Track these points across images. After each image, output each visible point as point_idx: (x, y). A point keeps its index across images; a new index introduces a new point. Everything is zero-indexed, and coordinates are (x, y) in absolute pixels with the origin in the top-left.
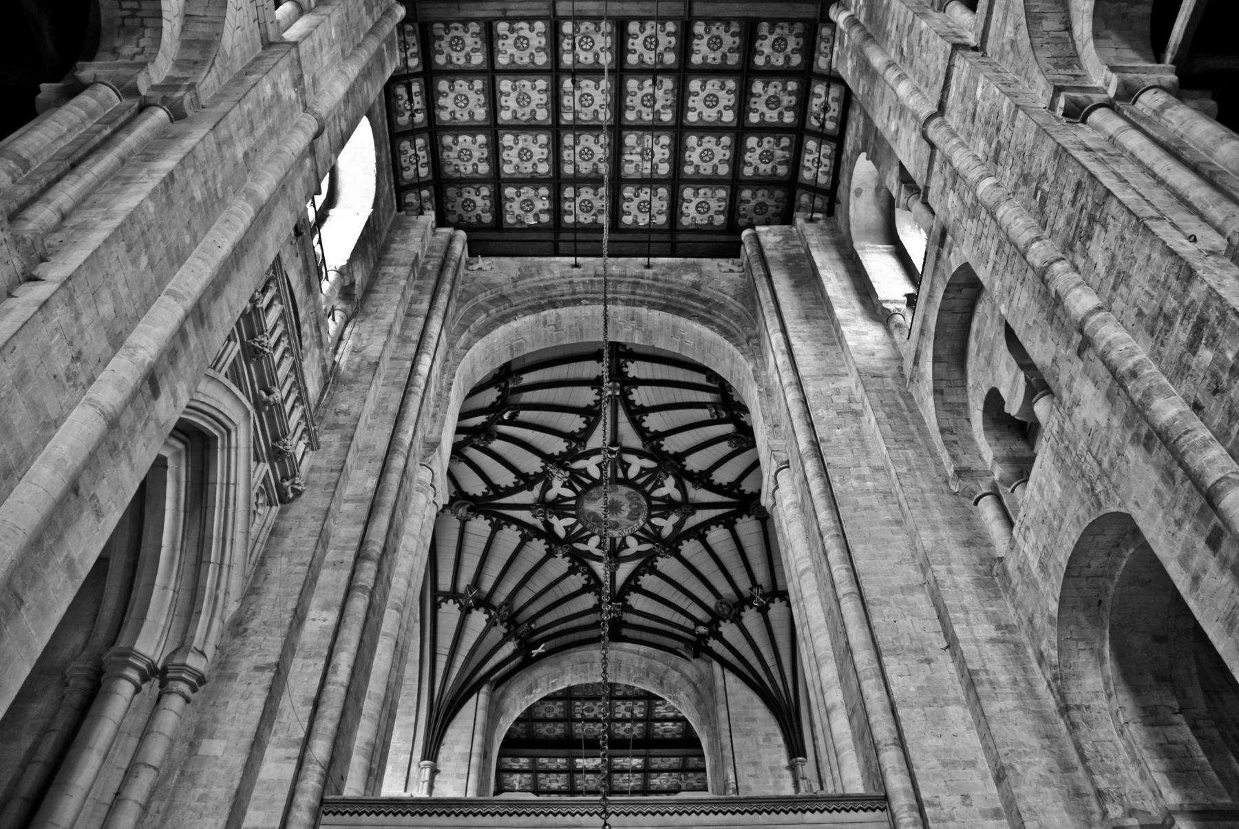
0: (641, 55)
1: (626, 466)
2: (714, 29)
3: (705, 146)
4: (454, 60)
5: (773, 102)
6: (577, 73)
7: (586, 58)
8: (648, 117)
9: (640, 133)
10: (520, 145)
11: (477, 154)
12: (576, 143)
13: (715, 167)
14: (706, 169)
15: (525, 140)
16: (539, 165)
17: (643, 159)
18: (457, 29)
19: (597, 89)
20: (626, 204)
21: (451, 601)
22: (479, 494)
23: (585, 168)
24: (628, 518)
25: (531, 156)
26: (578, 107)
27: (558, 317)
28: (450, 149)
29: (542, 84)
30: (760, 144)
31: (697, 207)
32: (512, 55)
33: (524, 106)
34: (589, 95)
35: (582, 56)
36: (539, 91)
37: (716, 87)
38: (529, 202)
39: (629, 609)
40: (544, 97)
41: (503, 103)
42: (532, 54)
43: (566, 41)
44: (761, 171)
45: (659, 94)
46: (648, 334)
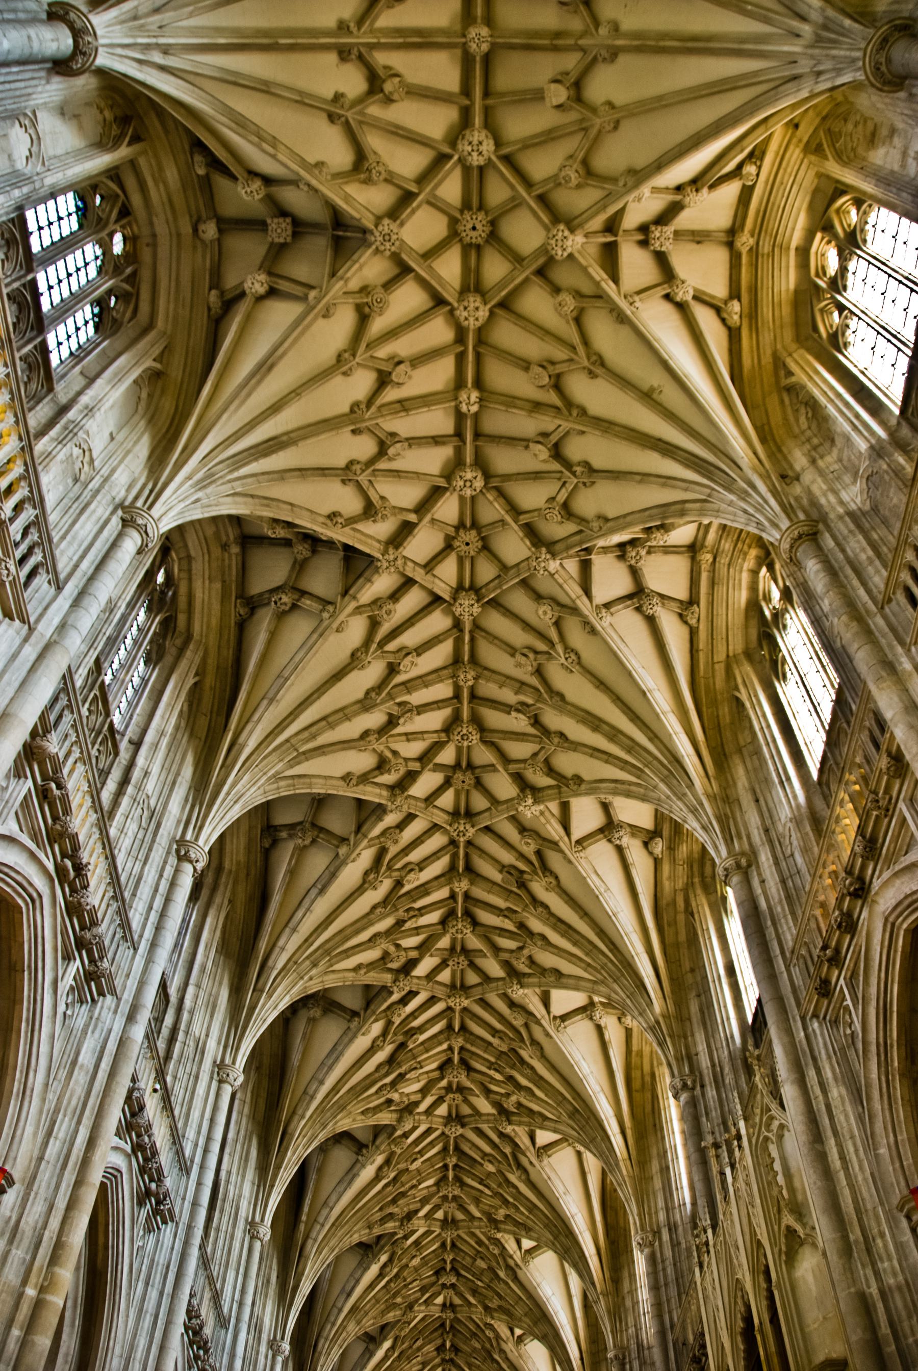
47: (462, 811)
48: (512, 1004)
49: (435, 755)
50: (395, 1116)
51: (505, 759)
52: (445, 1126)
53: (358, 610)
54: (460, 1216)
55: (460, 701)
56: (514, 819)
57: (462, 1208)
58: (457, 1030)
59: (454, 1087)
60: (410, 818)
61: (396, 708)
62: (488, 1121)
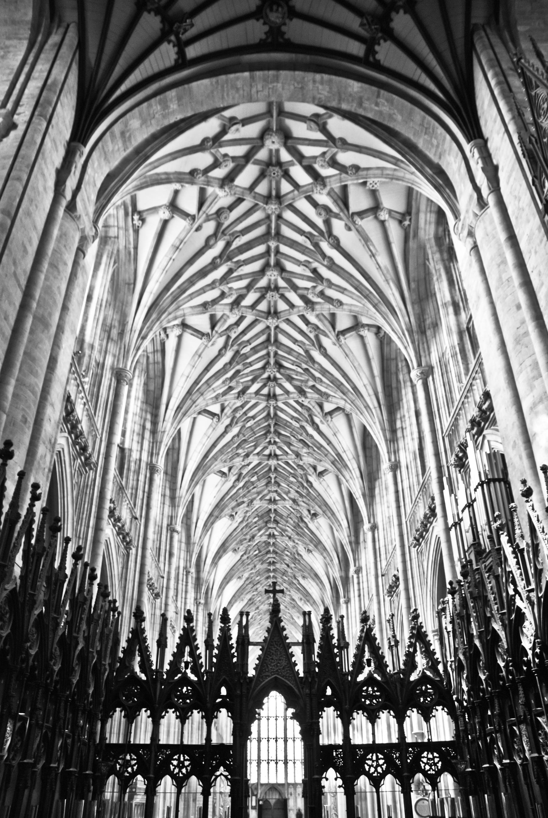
21: (377, 48)
47: (272, 311)
48: (302, 405)
49: (257, 306)
50: (241, 459)
51: (295, 288)
52: (268, 460)
53: (207, 220)
54: (277, 498)
55: (270, 256)
56: (303, 318)
57: (279, 495)
58: (272, 415)
59: (272, 441)
60: (242, 318)
61: (233, 265)
62: (291, 459)
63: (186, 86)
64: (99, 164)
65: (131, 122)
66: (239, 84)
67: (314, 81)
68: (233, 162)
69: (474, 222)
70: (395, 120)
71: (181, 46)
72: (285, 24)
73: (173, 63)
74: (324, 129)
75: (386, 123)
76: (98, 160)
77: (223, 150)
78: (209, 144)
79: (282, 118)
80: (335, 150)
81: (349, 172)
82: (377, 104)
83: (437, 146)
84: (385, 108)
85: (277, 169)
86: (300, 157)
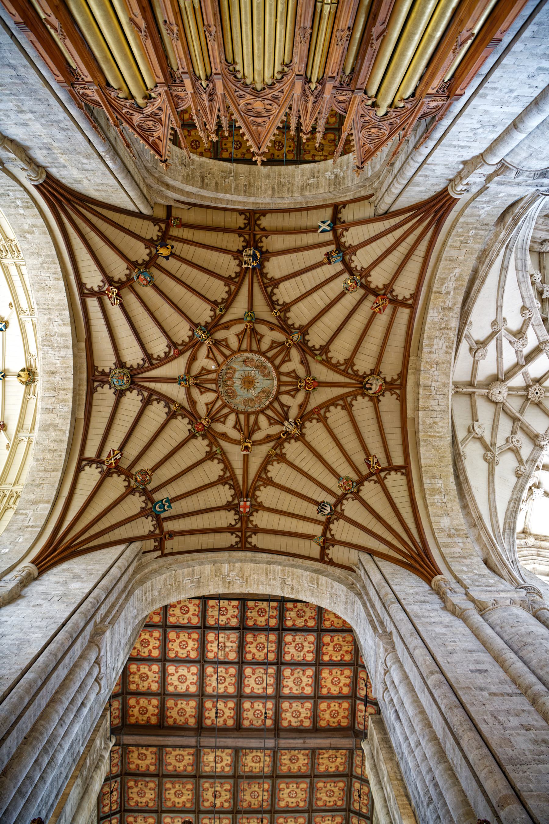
0: (226, 707)
1: (237, 426)
2: (183, 720)
3: (185, 651)
4: (337, 705)
5: (144, 677)
6: (264, 697)
7: (259, 705)
8: (221, 670)
9: (226, 660)
10: (302, 653)
11: (330, 648)
12: (267, 654)
13: (178, 637)
14: (184, 636)
15: (299, 657)
16: (291, 641)
17: (224, 644)
18: (334, 722)
19: (253, 687)
20: (235, 614)
22: (360, 398)
23: (262, 638)
24: (235, 370)
25: (296, 647)
26: (265, 677)
27: (282, 589)
28: (347, 652)
29: (286, 691)
30: (150, 651)
31: (188, 611)
32: (302, 708)
33: (298, 678)
34: (258, 684)
35: (261, 707)
36: (288, 686)
37: (180, 687)
38: (299, 616)
39: (238, 254)
40: (285, 683)
41: (310, 679)
42: (291, 708)
43: (270, 715)
44: (148, 634)
45: (214, 684)
46: (217, 573)
63: (423, 469)
64: (467, 565)
65: (442, 525)
66: (429, 421)
67: (430, 352)
68: (515, 434)
69: (526, 174)
70: (461, 275)
71: (391, 468)
72: (384, 379)
73: (404, 477)
74: (482, 344)
75: (465, 284)
76: (462, 566)
77: (500, 441)
78: (489, 455)
79: (476, 383)
80: (503, 332)
81: (528, 316)
82: (448, 293)
83: (476, 229)
84: (451, 285)
85: (531, 390)
86: (517, 367)
